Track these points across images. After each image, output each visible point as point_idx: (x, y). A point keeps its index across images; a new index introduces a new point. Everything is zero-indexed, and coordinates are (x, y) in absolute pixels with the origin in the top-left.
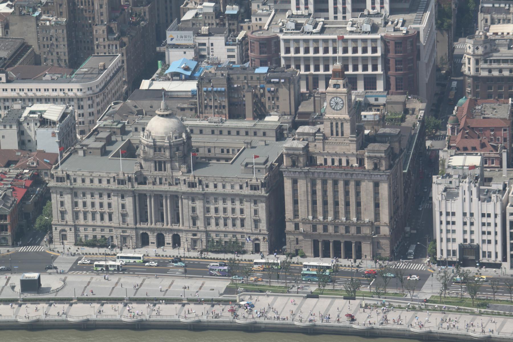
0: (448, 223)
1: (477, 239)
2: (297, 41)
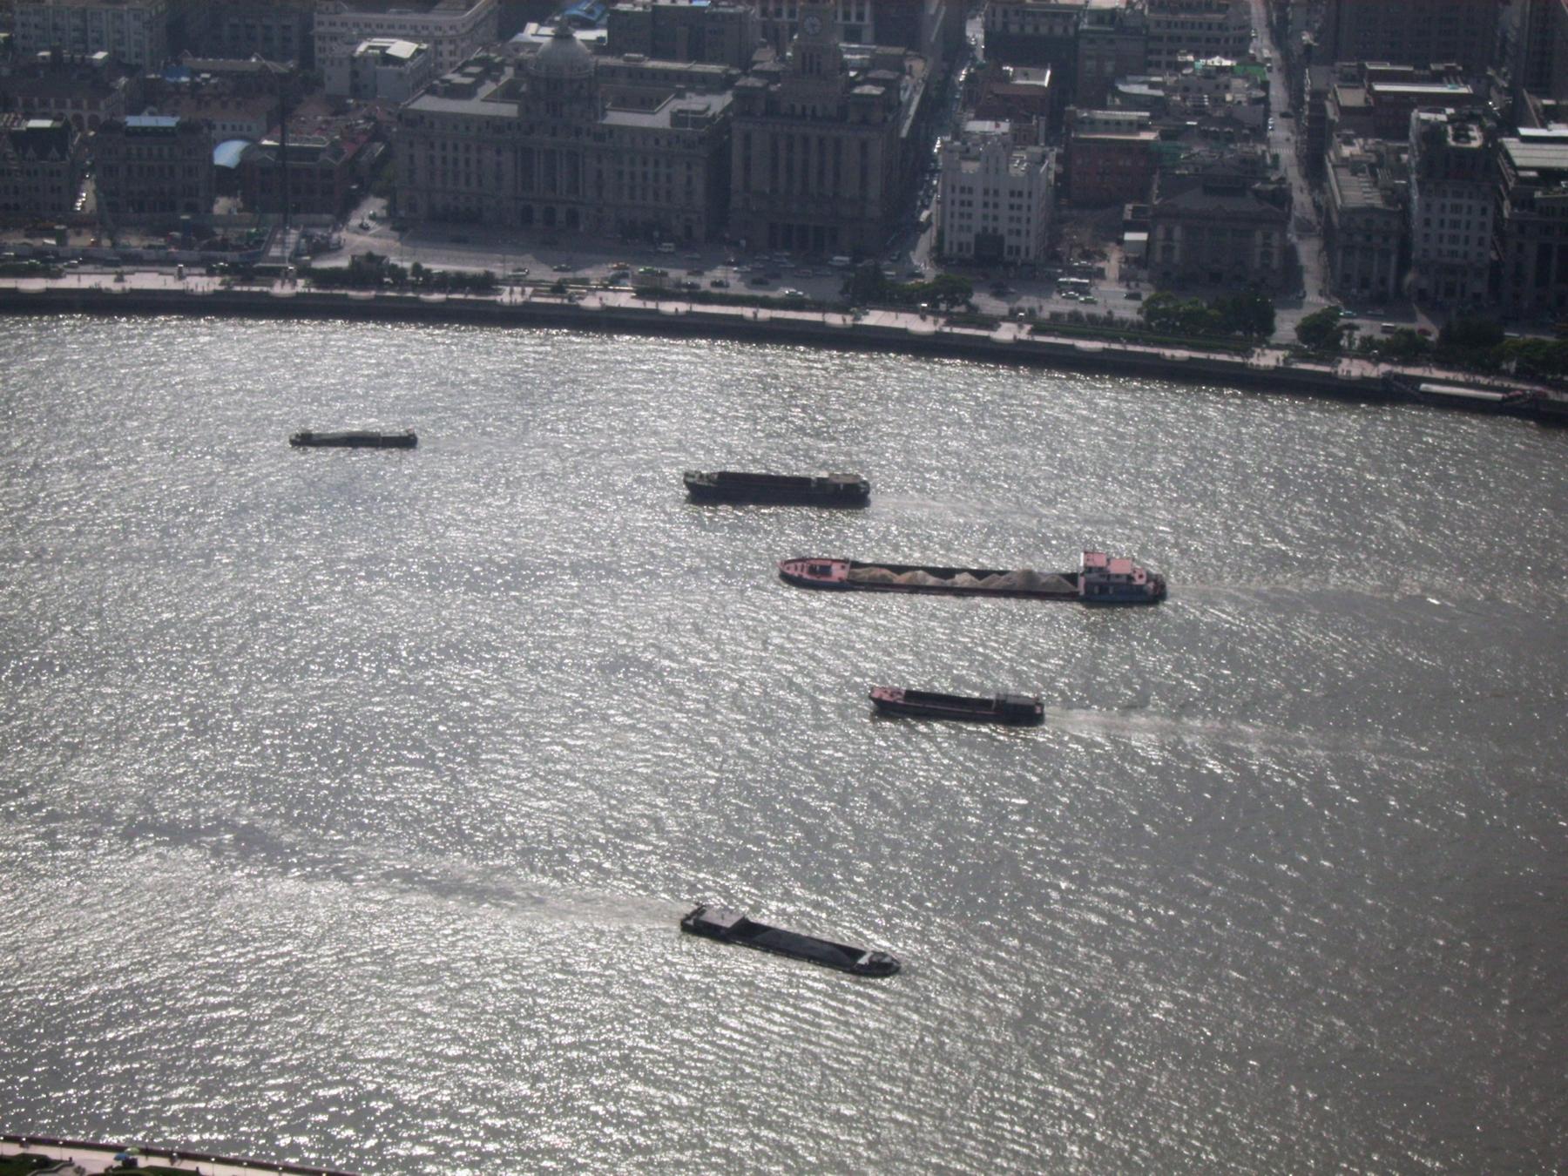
1: (1003, 227)
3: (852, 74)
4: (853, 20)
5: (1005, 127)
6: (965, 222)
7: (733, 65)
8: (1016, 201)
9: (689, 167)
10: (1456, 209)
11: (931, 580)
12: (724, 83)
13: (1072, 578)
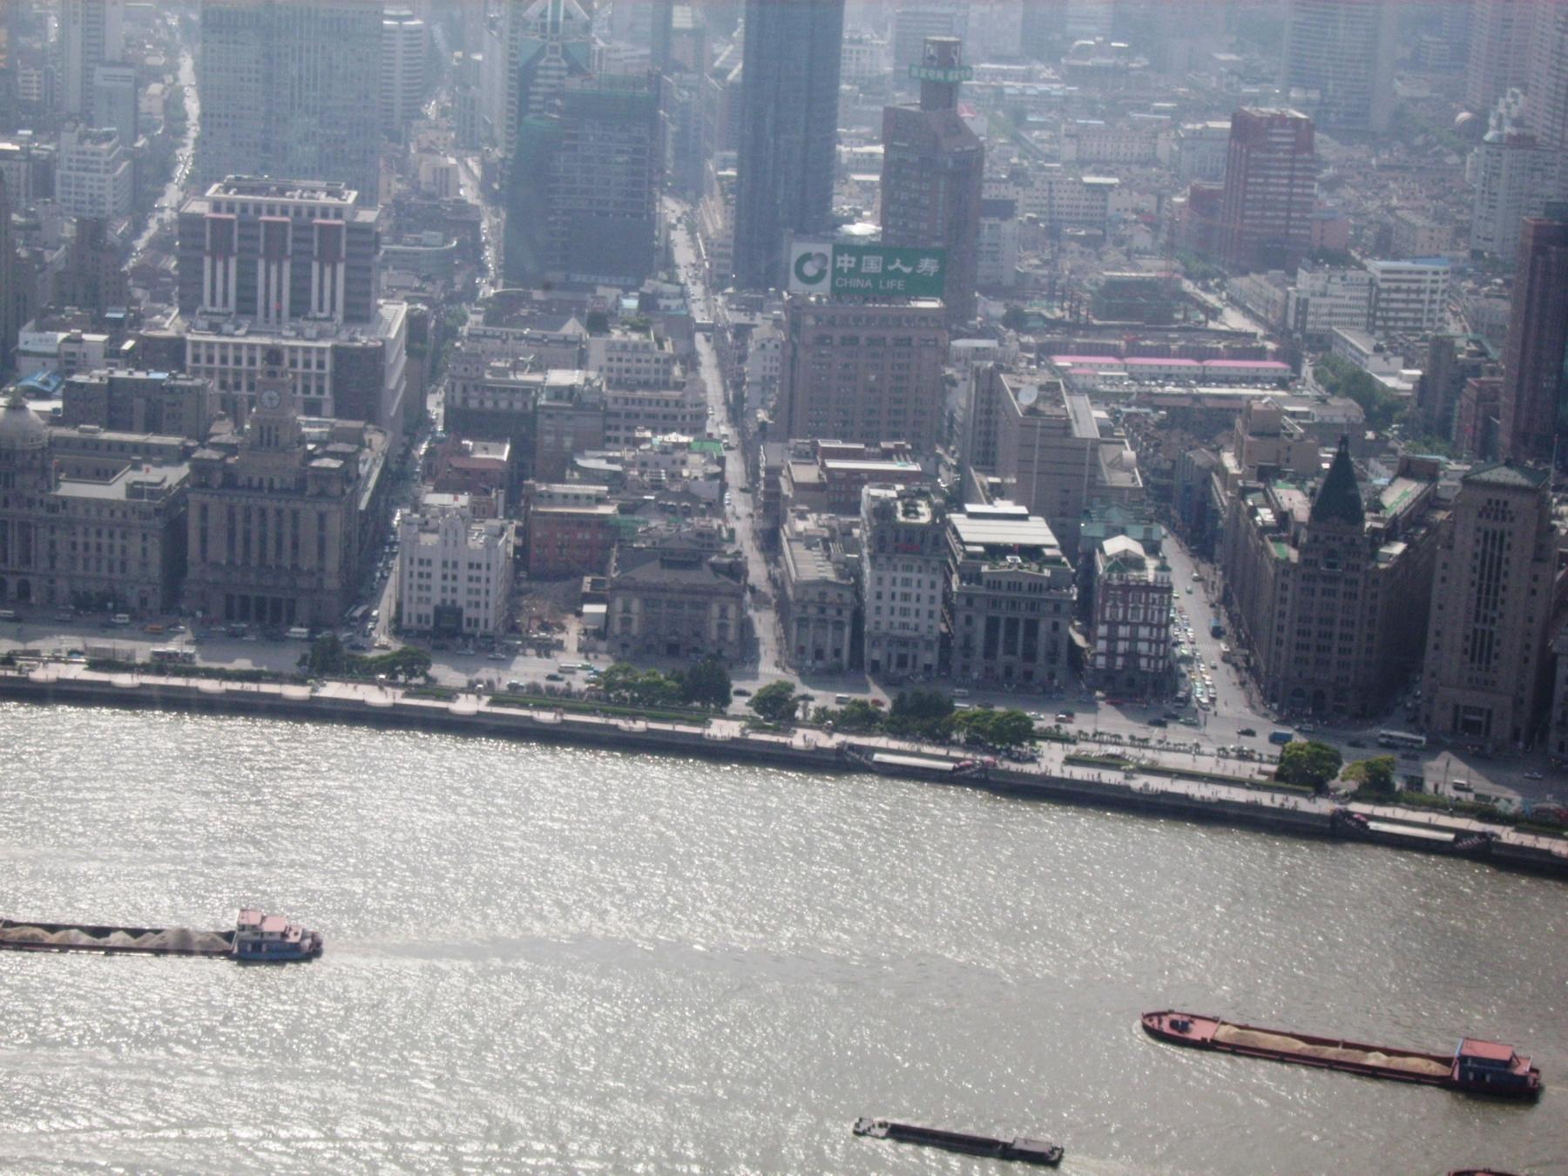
0: (421, 575)
1: (462, 600)
2: (210, 345)
3: (310, 447)
4: (313, 394)
5: (464, 499)
6: (424, 594)
7: (190, 437)
8: (474, 573)
9: (144, 538)
10: (906, 582)
11: (85, 939)
12: (184, 454)
13: (229, 936)
